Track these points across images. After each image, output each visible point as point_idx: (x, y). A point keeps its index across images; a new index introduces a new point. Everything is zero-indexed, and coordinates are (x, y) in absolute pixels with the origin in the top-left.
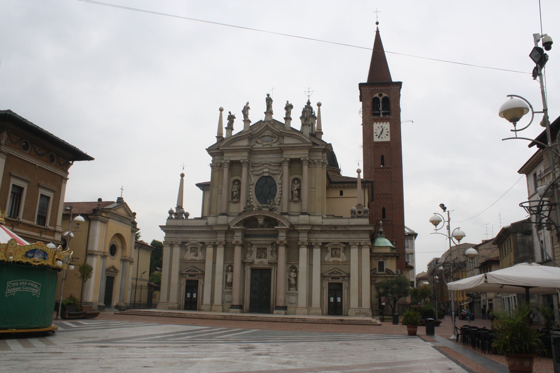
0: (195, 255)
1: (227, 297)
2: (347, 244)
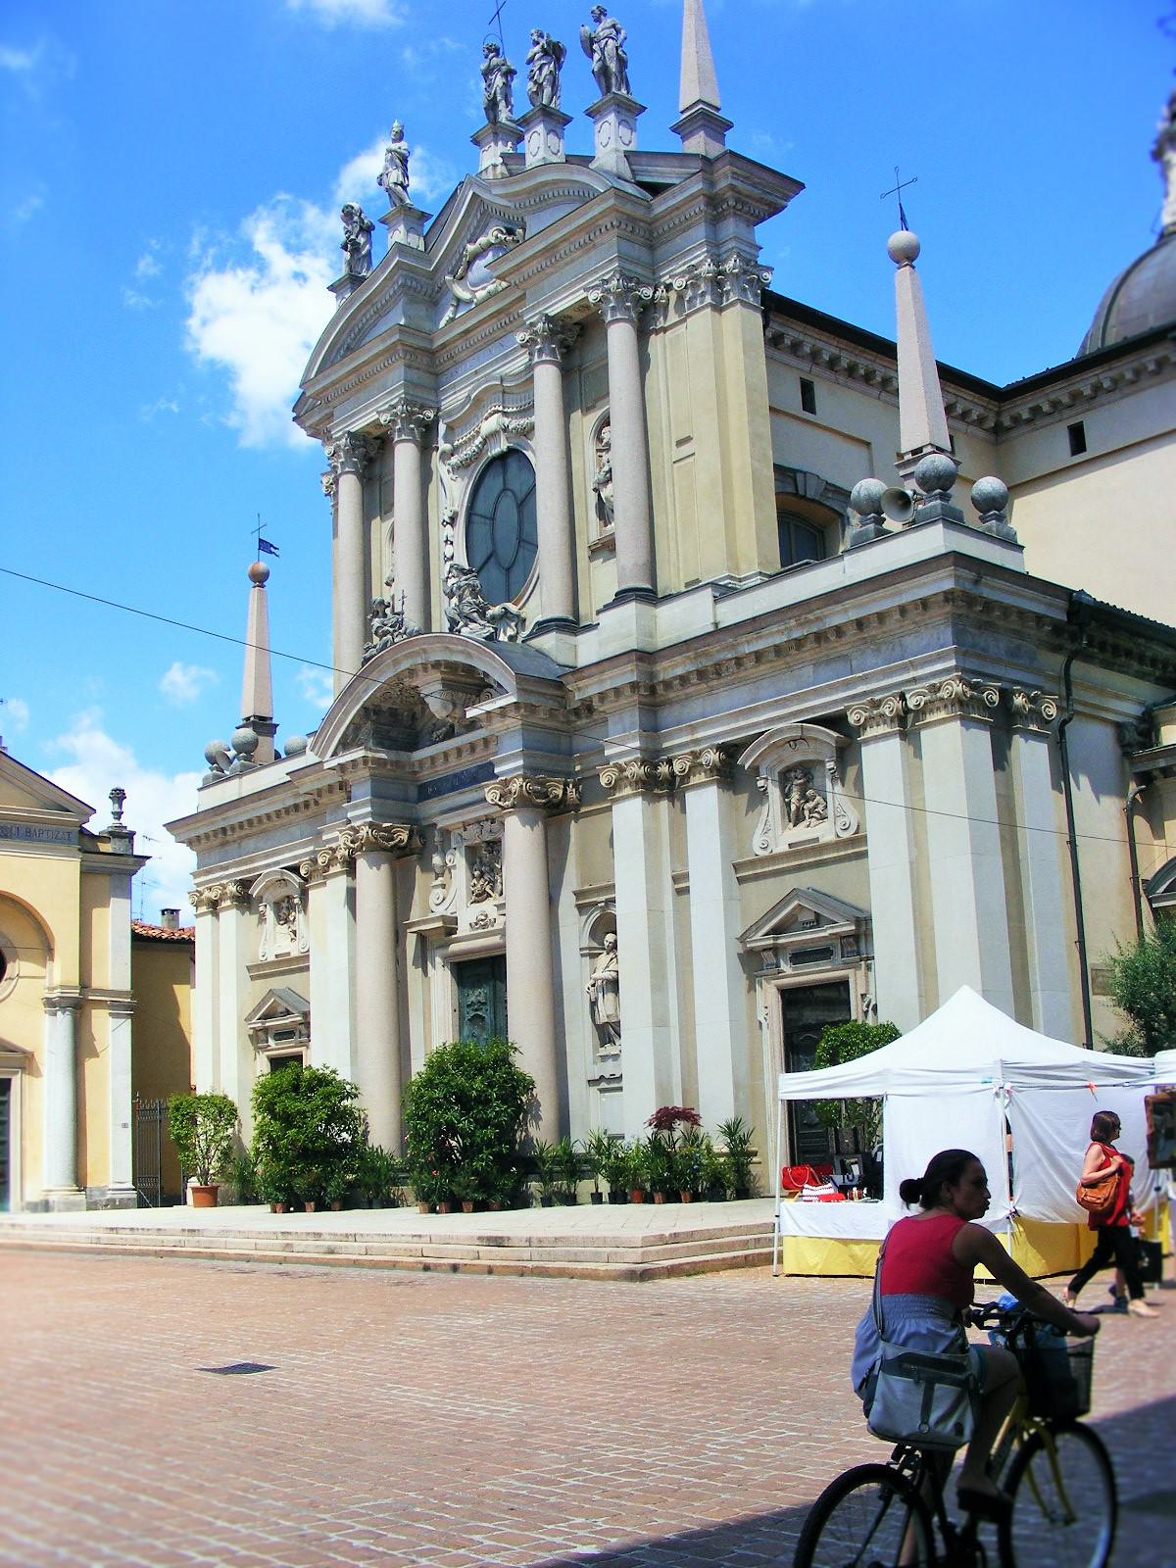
2: (836, 721)
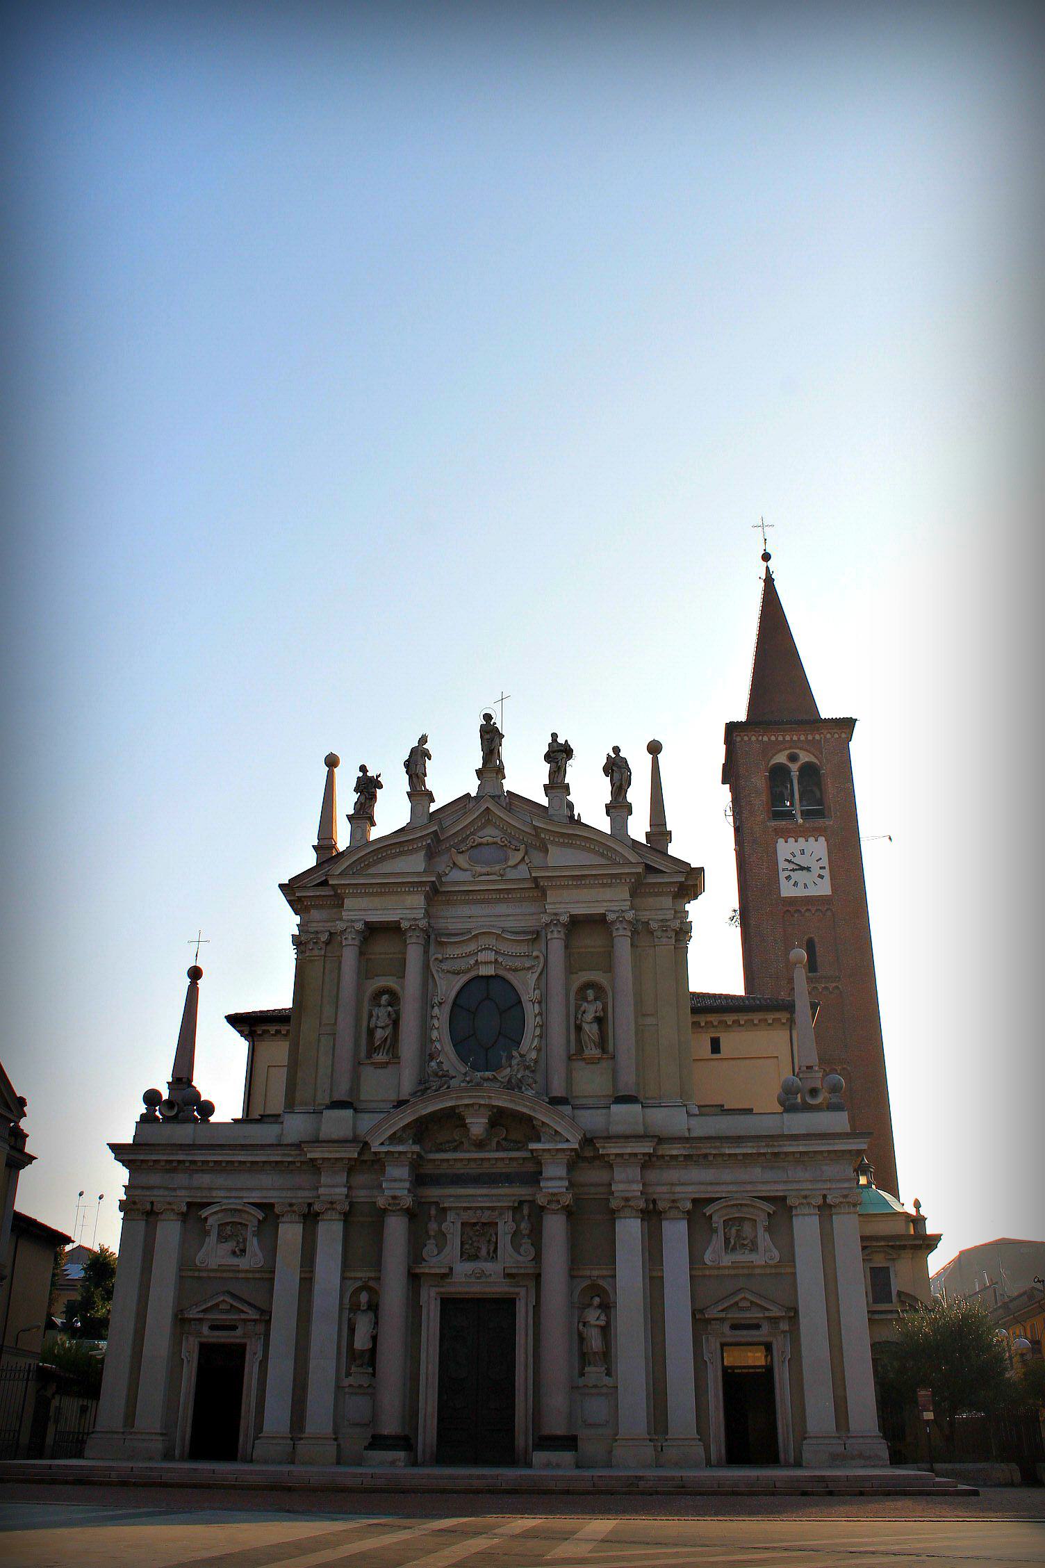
0: (234, 1253)
1: (357, 1406)
2: (779, 1201)
